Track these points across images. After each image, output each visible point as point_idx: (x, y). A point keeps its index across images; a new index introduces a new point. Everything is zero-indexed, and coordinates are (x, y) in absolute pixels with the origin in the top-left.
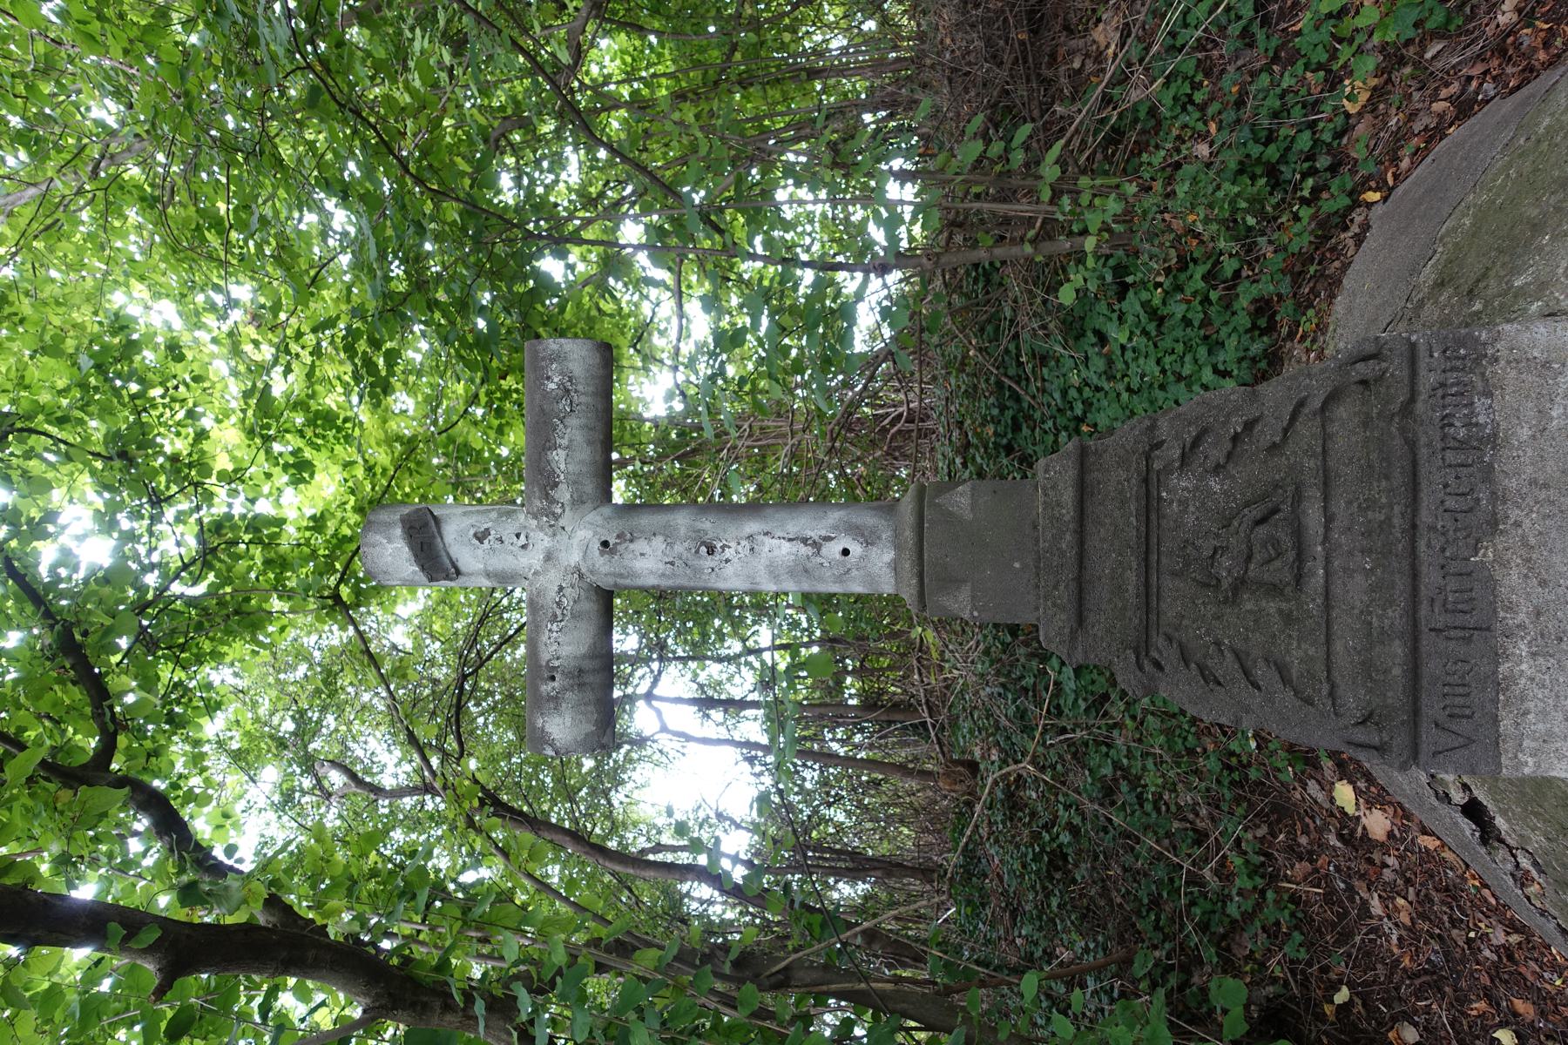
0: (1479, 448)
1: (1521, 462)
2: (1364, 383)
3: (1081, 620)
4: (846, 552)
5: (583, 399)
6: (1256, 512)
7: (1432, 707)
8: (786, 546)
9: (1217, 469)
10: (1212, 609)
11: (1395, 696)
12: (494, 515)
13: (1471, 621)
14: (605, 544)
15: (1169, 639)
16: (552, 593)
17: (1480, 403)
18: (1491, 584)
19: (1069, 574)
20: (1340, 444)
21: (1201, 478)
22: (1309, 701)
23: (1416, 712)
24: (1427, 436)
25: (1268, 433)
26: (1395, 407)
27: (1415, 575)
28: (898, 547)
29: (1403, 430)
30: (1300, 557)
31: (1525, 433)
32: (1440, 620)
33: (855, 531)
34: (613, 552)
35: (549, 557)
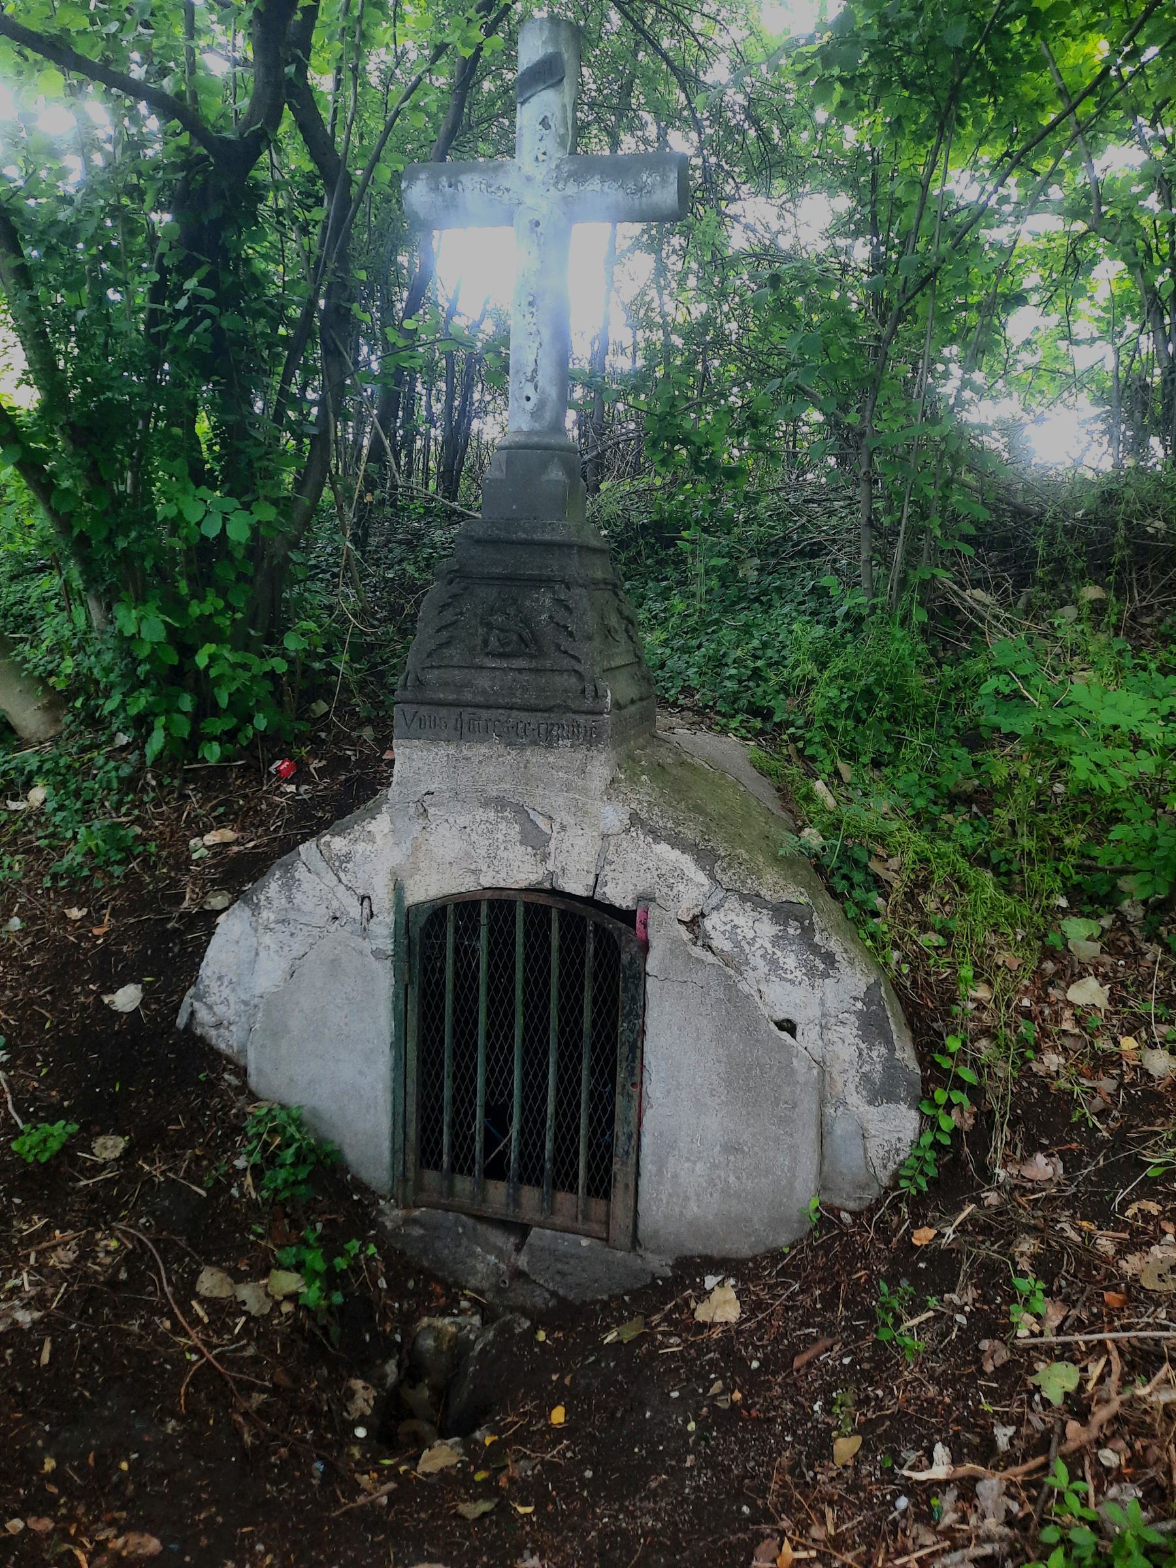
0: (548, 741)
1: (535, 756)
2: (583, 691)
3: (478, 541)
4: (528, 399)
5: (637, 202)
6: (526, 633)
7: (424, 711)
8: (532, 358)
9: (551, 617)
10: (479, 611)
11: (430, 695)
12: (562, 131)
13: (465, 730)
14: (537, 224)
15: (465, 589)
16: (506, 184)
17: (568, 742)
18: (482, 741)
19: (503, 535)
20: (557, 678)
21: (549, 610)
22: (430, 655)
23: (422, 703)
24: (554, 717)
25: (565, 644)
26: (569, 702)
27: (488, 707)
28: (530, 433)
29: (559, 706)
30: (502, 656)
31: (551, 759)
32: (466, 717)
33: (541, 405)
34: (532, 231)
35: (529, 179)
